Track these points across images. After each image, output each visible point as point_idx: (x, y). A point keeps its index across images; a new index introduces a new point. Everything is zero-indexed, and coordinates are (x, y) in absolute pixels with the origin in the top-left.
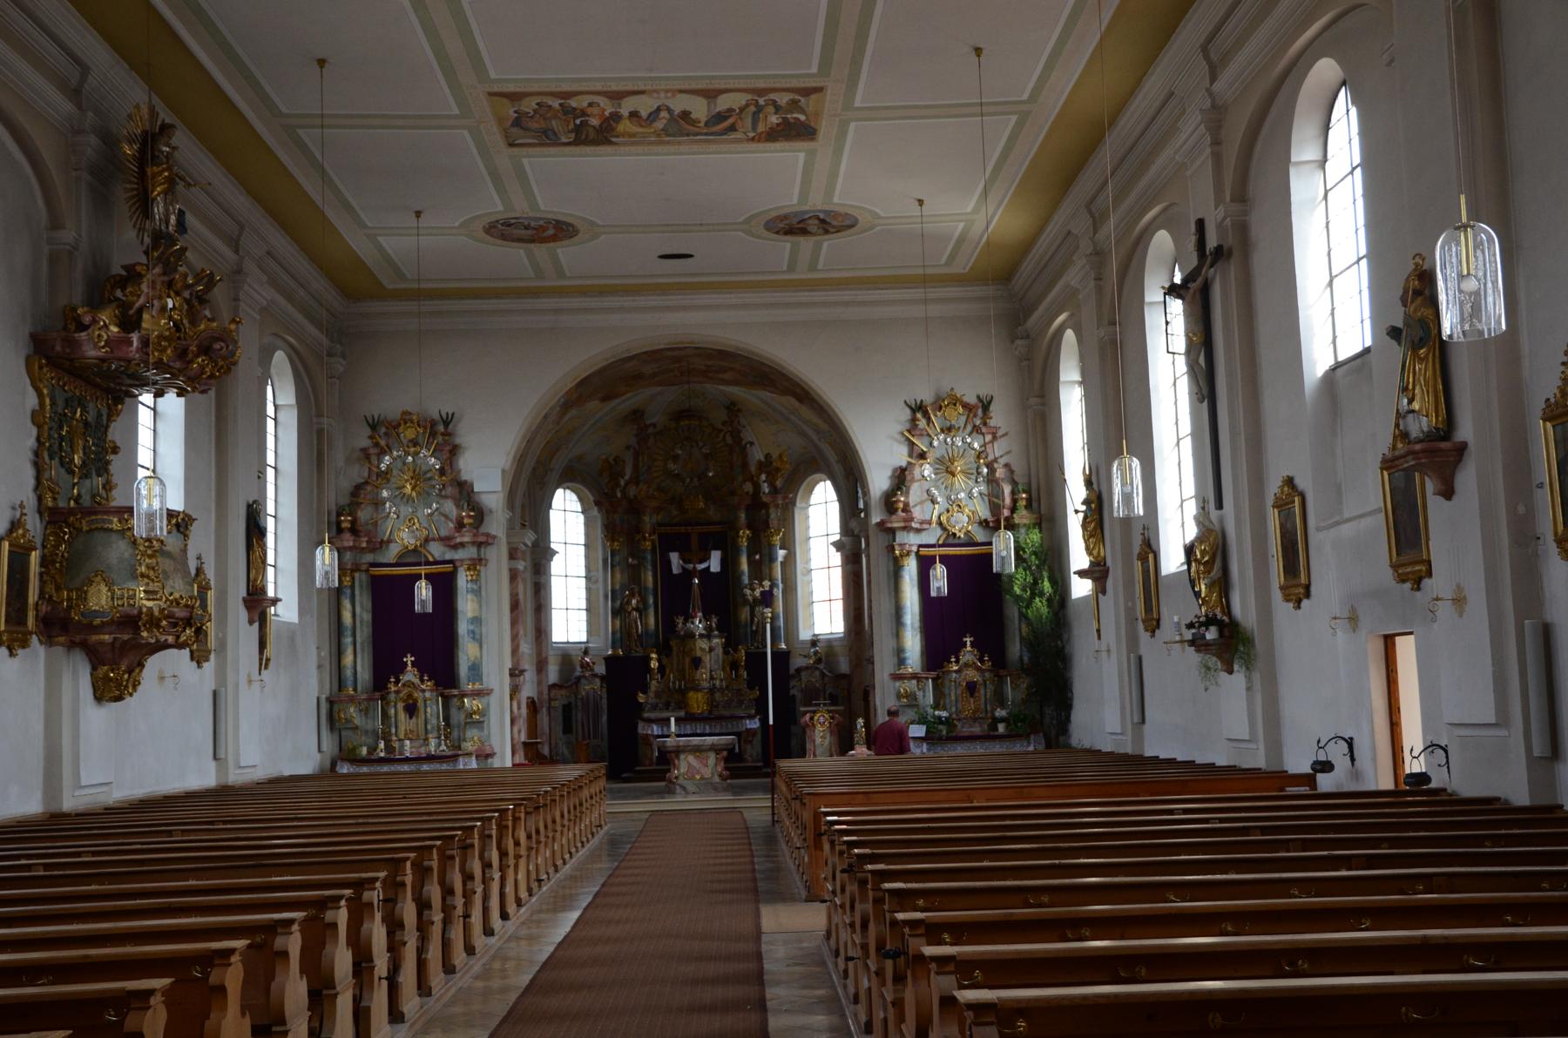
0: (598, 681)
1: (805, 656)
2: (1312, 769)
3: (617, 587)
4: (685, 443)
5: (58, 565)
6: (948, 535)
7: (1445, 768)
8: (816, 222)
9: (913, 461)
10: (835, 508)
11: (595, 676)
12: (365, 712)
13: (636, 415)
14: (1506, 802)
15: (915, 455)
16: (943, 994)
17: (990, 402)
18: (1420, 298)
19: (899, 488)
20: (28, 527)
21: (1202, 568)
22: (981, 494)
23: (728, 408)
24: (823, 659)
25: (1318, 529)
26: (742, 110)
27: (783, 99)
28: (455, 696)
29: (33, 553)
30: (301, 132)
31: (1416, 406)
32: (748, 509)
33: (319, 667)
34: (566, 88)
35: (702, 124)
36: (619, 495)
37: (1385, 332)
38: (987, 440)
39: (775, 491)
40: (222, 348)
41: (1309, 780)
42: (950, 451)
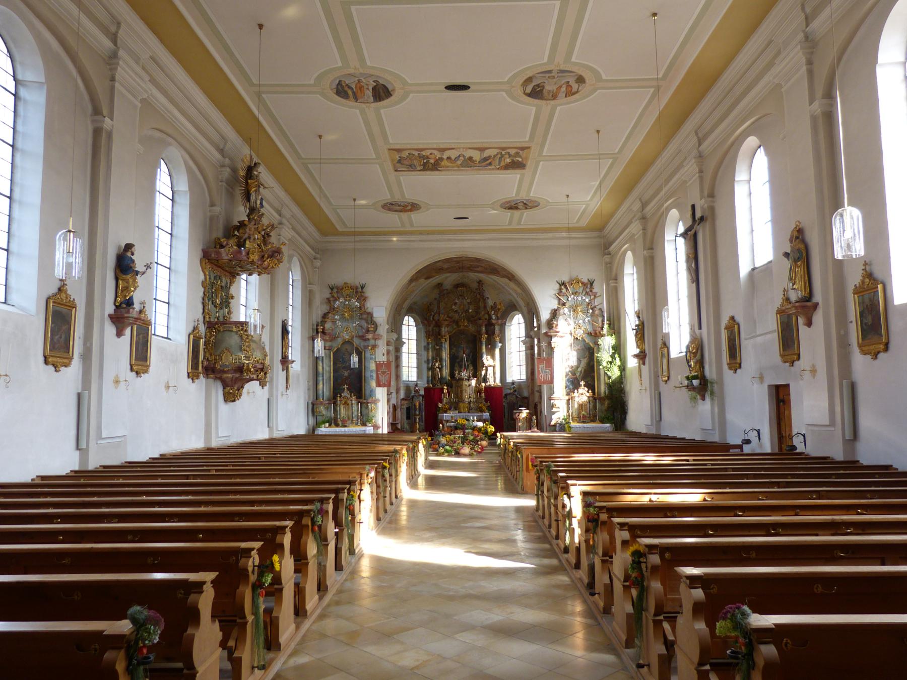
0: (421, 397)
1: (509, 389)
2: (742, 443)
3: (430, 358)
4: (460, 297)
5: (211, 345)
7: (803, 444)
8: (523, 204)
9: (560, 307)
10: (523, 326)
11: (420, 395)
12: (327, 409)
13: (439, 285)
14: (833, 459)
15: (561, 304)
16: (623, 539)
18: (798, 240)
19: (554, 318)
20: (200, 329)
21: (692, 355)
22: (589, 321)
23: (478, 283)
24: (517, 390)
25: (746, 339)
26: (495, 156)
27: (513, 152)
28: (364, 403)
29: (202, 340)
30: (309, 165)
31: (796, 286)
32: (486, 326)
33: (308, 389)
34: (421, 147)
35: (477, 162)
36: (431, 319)
37: (782, 254)
39: (498, 318)
40: (277, 256)
41: (740, 447)
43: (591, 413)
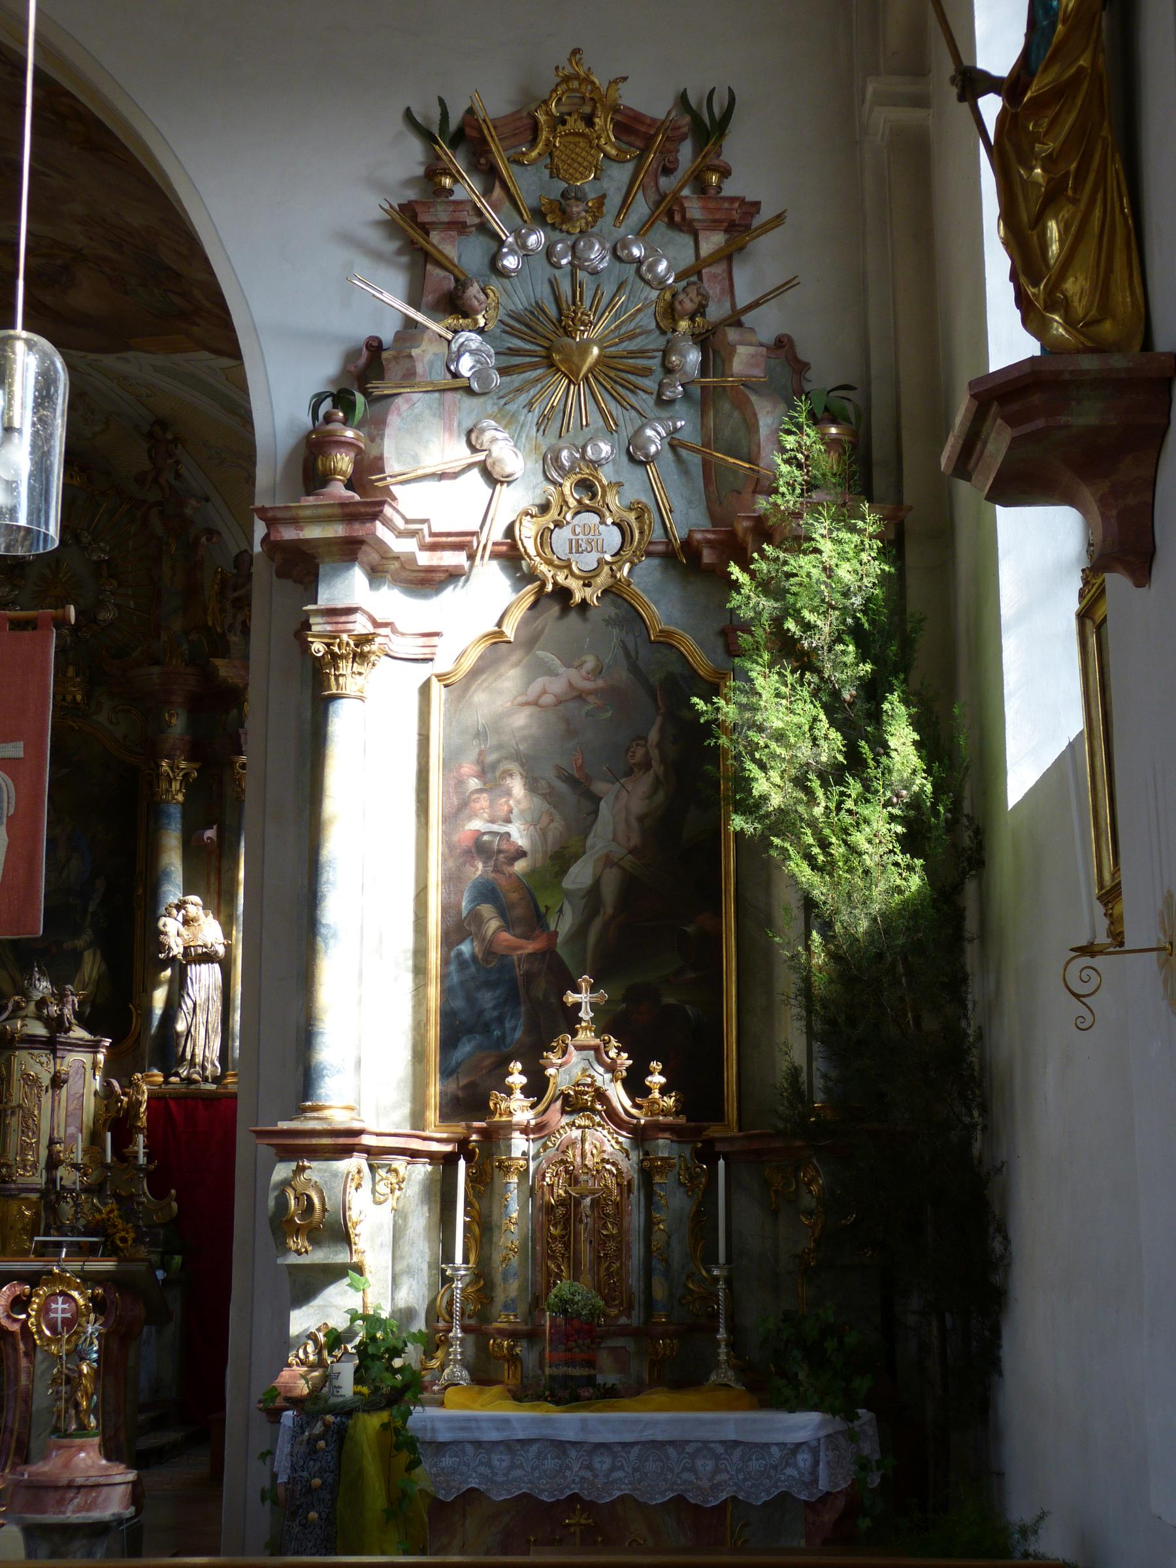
6: (540, 593)
15: (429, 298)
17: (722, 125)
22: (674, 444)
23: (150, 436)
38: (706, 249)
42: (565, 288)
43: (659, 1292)
